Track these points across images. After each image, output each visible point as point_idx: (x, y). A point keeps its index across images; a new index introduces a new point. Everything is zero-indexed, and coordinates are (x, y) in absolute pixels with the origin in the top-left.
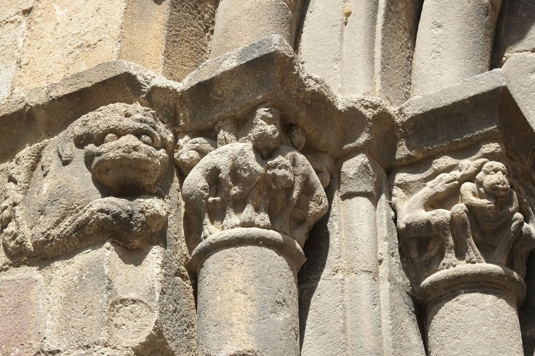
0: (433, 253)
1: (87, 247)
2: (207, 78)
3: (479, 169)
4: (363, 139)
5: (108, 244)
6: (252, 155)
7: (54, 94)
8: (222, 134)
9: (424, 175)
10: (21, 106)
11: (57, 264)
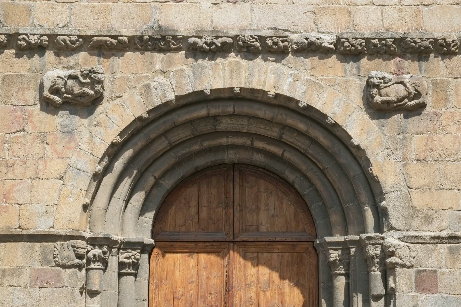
0: (124, 267)
1: (73, 268)
2: (96, 237)
3: (136, 254)
4: (117, 246)
5: (77, 269)
6: (102, 254)
7: (67, 234)
8: (96, 247)
9: (125, 252)
10: (60, 234)
11: (67, 269)
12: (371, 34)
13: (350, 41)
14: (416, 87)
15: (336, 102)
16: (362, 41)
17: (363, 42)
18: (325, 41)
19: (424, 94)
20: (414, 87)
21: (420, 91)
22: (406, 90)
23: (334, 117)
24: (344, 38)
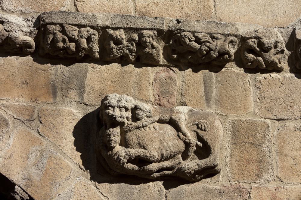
12: (110, 18)
13: (66, 29)
14: (199, 131)
15: (34, 155)
16: (92, 31)
17: (94, 35)
18: (15, 27)
19: (216, 148)
20: (195, 131)
21: (209, 141)
22: (179, 136)
23: (28, 187)
24: (55, 24)
